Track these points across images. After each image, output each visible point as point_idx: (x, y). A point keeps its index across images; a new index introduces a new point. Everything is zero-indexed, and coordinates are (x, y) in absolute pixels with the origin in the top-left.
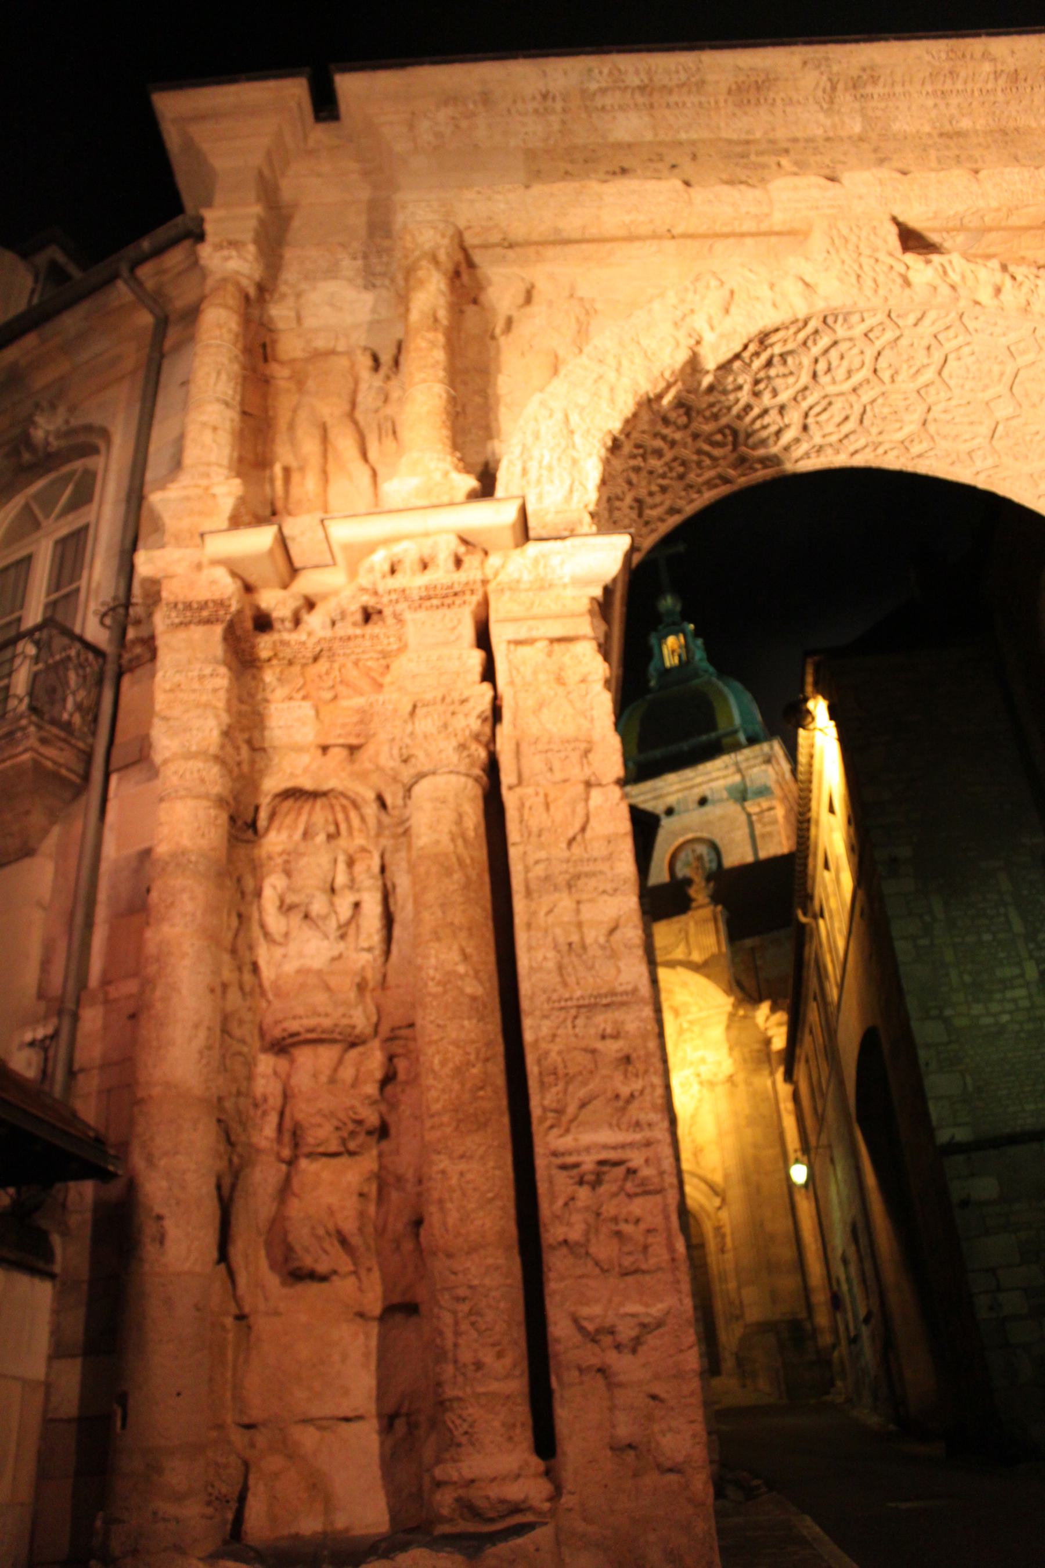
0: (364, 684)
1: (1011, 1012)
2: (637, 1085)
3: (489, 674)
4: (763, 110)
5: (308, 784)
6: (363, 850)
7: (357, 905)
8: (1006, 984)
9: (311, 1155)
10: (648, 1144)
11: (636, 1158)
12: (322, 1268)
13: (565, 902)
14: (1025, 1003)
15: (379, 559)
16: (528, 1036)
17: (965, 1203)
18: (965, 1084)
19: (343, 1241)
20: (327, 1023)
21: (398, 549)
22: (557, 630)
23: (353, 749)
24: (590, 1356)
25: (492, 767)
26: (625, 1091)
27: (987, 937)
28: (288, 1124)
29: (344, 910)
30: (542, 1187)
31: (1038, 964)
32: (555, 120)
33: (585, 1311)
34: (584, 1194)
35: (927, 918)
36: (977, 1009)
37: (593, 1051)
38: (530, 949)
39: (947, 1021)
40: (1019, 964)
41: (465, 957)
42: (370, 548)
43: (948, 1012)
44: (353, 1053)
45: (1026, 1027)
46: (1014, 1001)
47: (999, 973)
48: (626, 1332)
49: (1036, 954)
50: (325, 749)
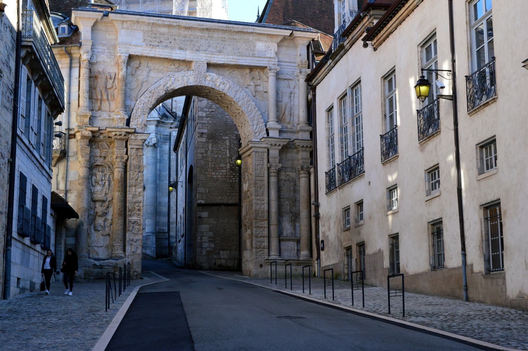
0: (107, 147)
1: (221, 175)
2: (140, 213)
3: (127, 154)
4: (190, 31)
5: (99, 164)
6: (106, 174)
7: (105, 182)
8: (222, 168)
9: (99, 216)
10: (140, 220)
11: (139, 221)
12: (99, 229)
13: (134, 188)
14: (225, 174)
15: (114, 133)
16: (127, 205)
17: (200, 217)
18: (206, 191)
19: (102, 227)
20: (101, 199)
21: (117, 133)
22: (137, 147)
23: (105, 157)
24: (130, 242)
25: (126, 166)
26: (138, 213)
27: (220, 156)
28: (96, 212)
29: (103, 183)
30: (127, 224)
31: (230, 165)
32: (150, 27)
33: (131, 237)
34: (132, 225)
35: (207, 149)
36: (213, 173)
37: (135, 208)
38: (129, 194)
39: (205, 175)
40: (225, 164)
41: (121, 194)
42: (112, 132)
43: (207, 173)
44: (104, 203)
45: (223, 179)
46: (222, 173)
47: (221, 165)
48: (135, 240)
49: (230, 162)
50: (101, 157)
